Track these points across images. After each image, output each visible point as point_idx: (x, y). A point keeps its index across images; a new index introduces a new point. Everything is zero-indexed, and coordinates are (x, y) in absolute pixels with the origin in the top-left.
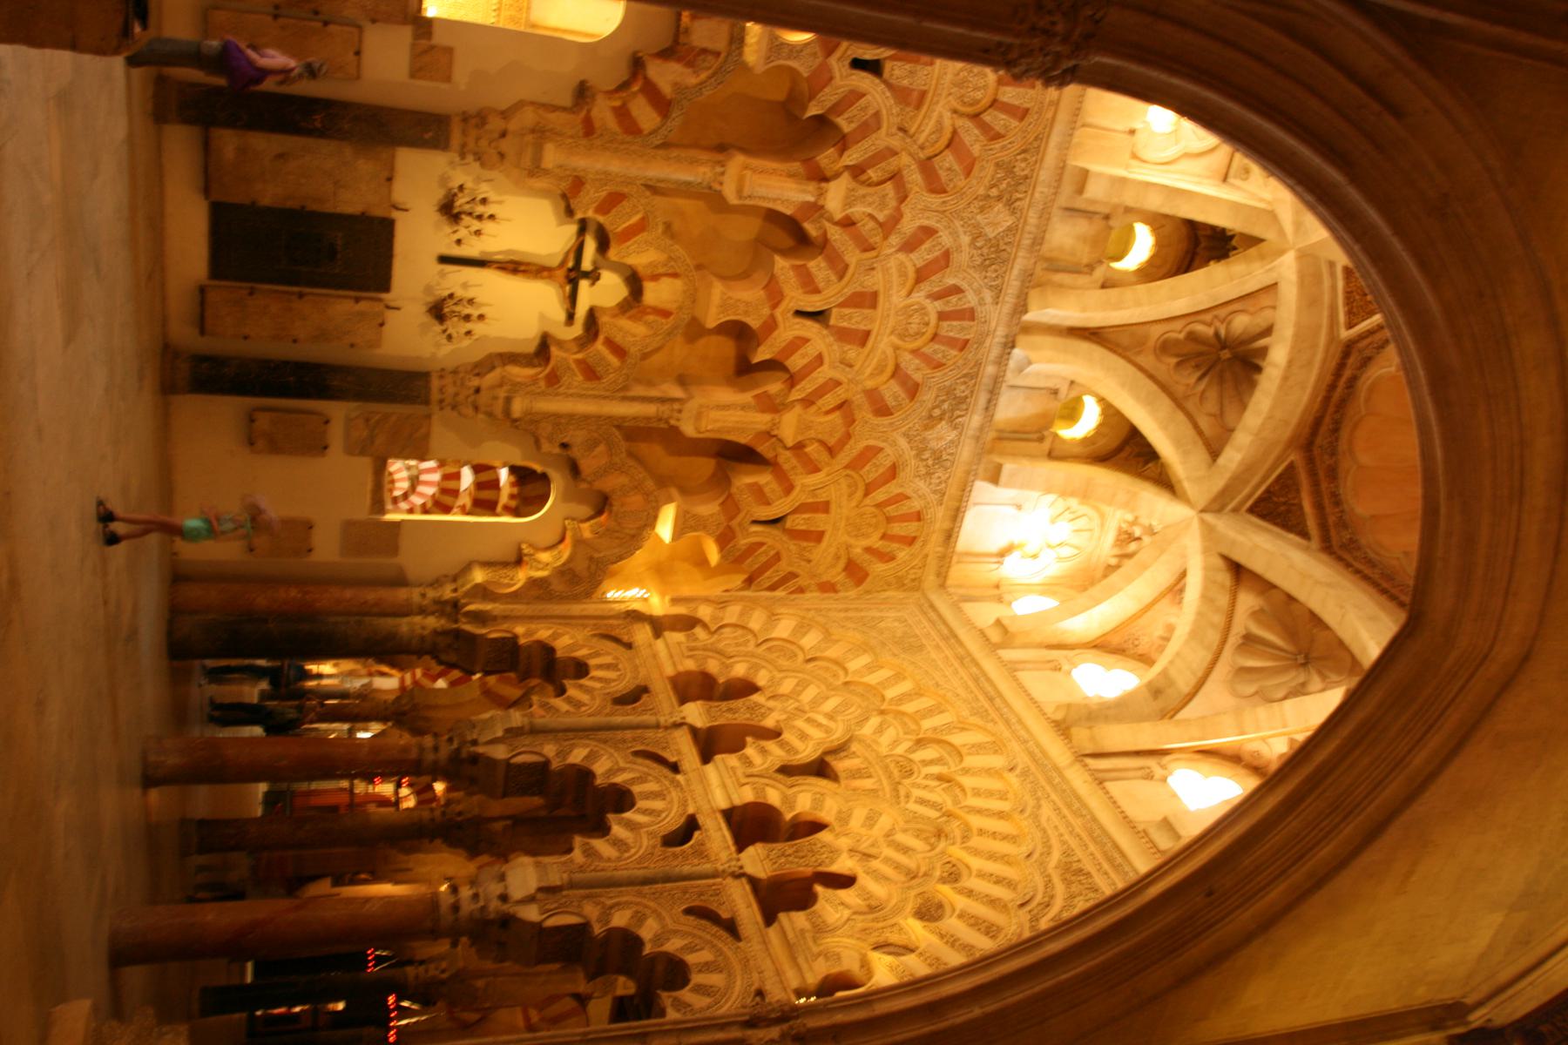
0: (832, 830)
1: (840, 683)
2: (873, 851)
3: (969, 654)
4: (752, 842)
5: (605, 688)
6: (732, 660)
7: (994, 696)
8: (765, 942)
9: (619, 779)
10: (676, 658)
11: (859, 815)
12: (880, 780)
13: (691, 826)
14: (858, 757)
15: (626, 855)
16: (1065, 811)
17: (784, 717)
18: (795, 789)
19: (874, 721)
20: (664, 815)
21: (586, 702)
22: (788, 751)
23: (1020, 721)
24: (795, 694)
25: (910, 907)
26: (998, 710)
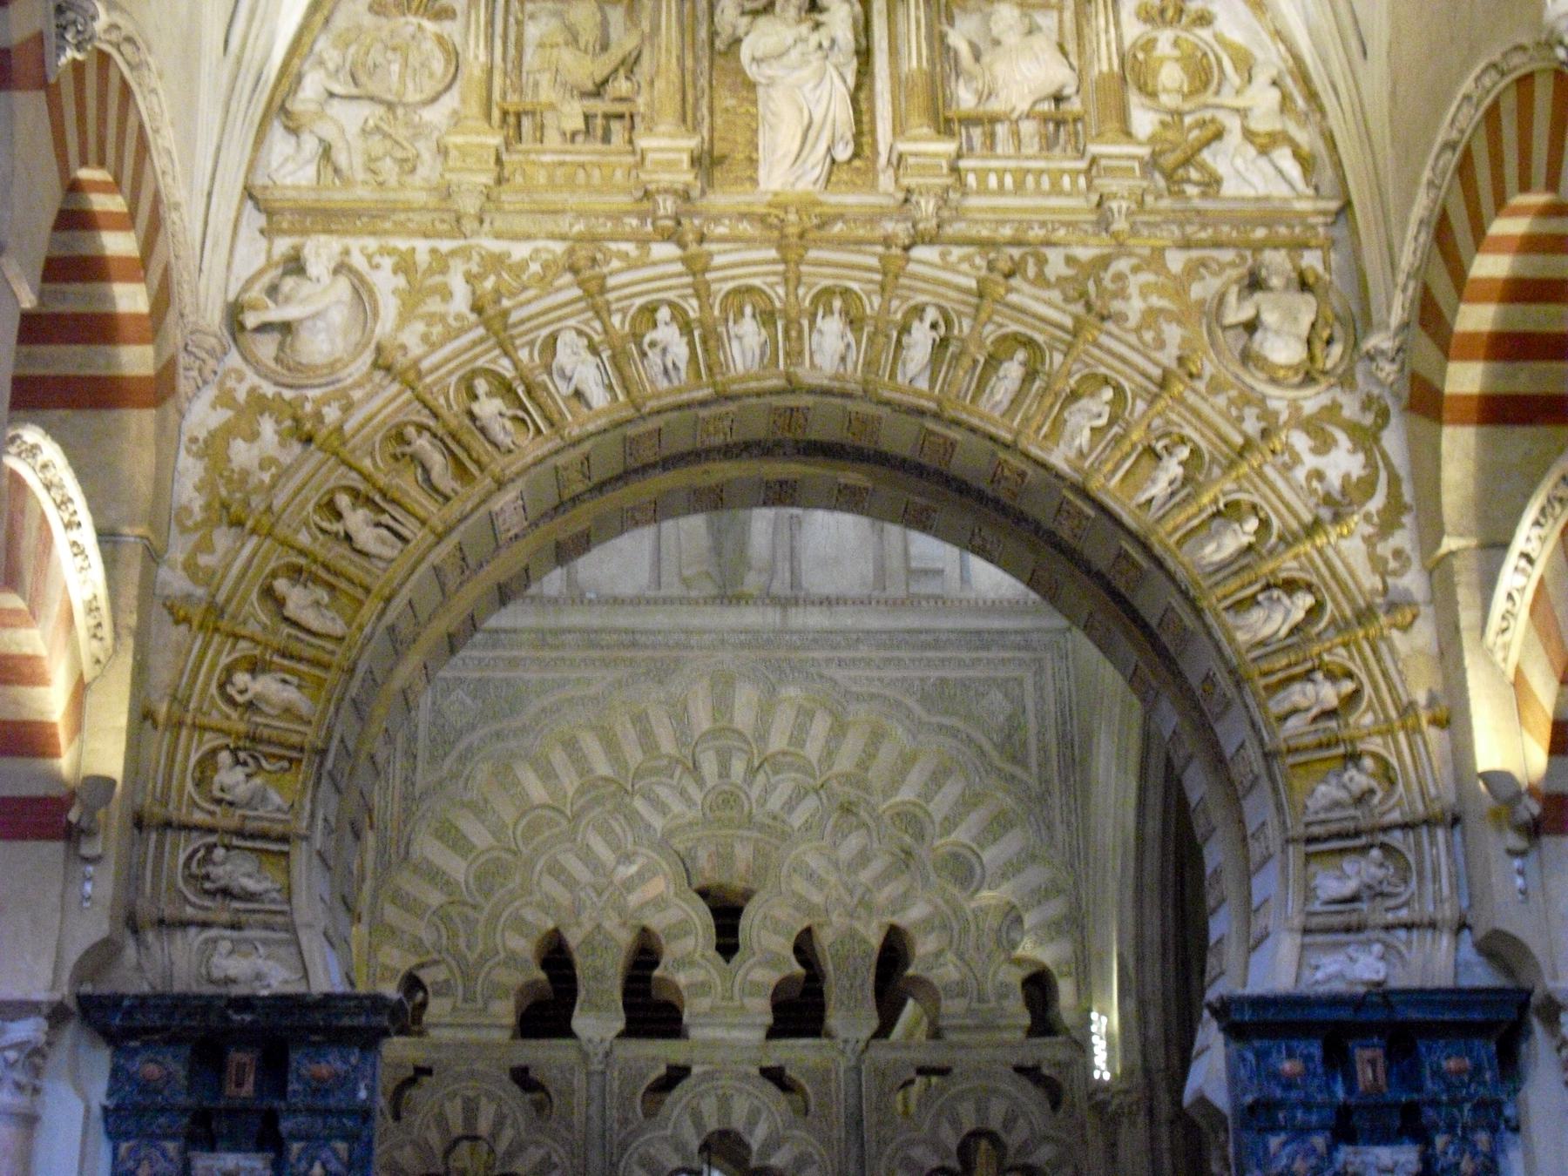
0: (821, 926)
1: (564, 823)
2: (859, 892)
3: (541, 632)
4: (821, 1019)
5: (515, 1120)
6: (500, 947)
7: (632, 640)
8: (963, 1046)
9: (695, 1144)
10: (487, 1022)
11: (800, 885)
12: (742, 839)
13: (775, 1076)
14: (695, 847)
15: (816, 1157)
16: (844, 654)
17: (613, 914)
18: (755, 946)
19: (639, 804)
20: (756, 1102)
21: (542, 1152)
22: (687, 933)
23: (687, 632)
24: (570, 883)
25: (955, 890)
26: (654, 647)
